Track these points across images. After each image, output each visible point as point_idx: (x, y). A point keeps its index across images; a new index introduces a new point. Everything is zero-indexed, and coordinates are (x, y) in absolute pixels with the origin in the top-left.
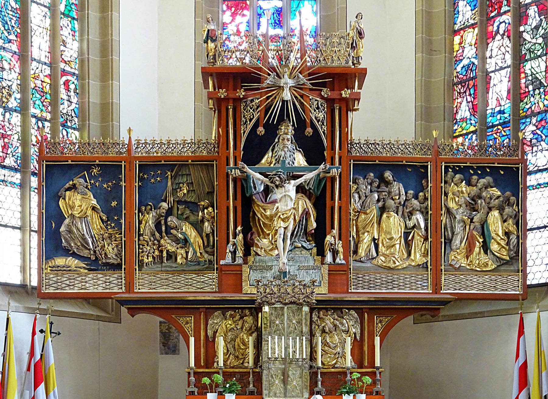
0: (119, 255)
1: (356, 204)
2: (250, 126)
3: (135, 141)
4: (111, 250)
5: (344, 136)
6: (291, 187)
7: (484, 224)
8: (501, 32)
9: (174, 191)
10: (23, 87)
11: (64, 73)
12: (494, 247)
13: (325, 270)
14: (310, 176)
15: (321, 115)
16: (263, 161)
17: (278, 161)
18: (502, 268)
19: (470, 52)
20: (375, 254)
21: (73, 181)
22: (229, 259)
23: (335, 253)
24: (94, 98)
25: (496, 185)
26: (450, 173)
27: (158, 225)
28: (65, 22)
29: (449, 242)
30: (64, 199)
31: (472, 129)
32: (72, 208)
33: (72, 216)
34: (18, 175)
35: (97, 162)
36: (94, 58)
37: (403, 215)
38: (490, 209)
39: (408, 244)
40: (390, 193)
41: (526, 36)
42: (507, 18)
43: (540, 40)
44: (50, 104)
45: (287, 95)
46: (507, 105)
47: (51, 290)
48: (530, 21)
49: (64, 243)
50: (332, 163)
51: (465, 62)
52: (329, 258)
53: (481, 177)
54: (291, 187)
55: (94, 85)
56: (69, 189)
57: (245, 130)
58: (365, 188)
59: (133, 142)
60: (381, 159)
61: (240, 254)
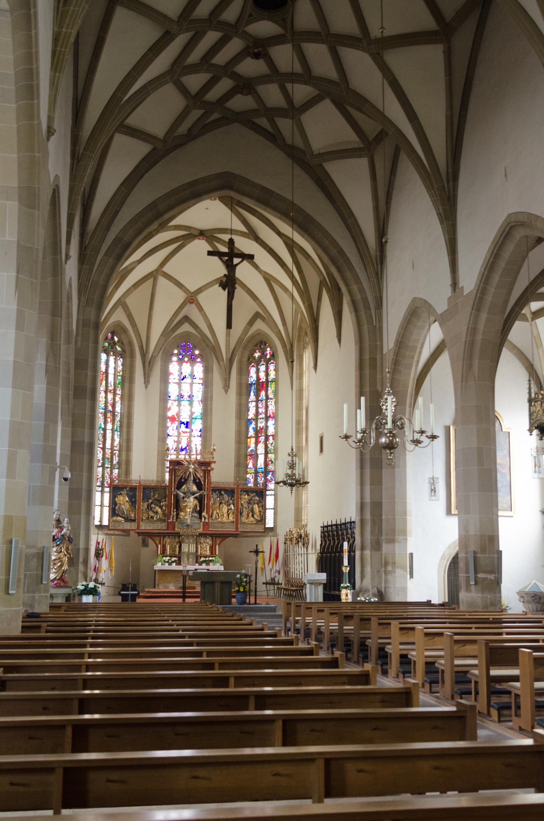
0: (135, 517)
1: (212, 501)
2: (179, 478)
4: (133, 515)
5: (209, 480)
6: (192, 499)
7: (252, 509)
8: (262, 442)
9: (154, 496)
10: (104, 458)
11: (115, 450)
12: (255, 516)
13: (202, 524)
14: (197, 495)
15: (201, 475)
16: (183, 488)
17: (188, 488)
18: (258, 523)
19: (252, 446)
20: (217, 517)
22: (171, 520)
23: (205, 518)
24: (124, 458)
25: (257, 495)
26: (242, 492)
27: (148, 507)
28: (116, 433)
29: (241, 514)
31: (253, 472)
32: (120, 501)
33: (120, 504)
34: (100, 488)
36: (124, 444)
37: (227, 506)
38: (254, 504)
39: (228, 515)
40: (223, 498)
41: (269, 446)
42: (263, 438)
43: (273, 448)
44: (110, 462)
45: (191, 470)
46: (263, 466)
47: (112, 528)
48: (270, 441)
49: (117, 513)
50: (205, 490)
51: (251, 449)
52: (203, 520)
53: (252, 493)
54: (192, 499)
55: (124, 453)
57: (178, 479)
58: (215, 496)
60: (221, 488)
61: (175, 518)
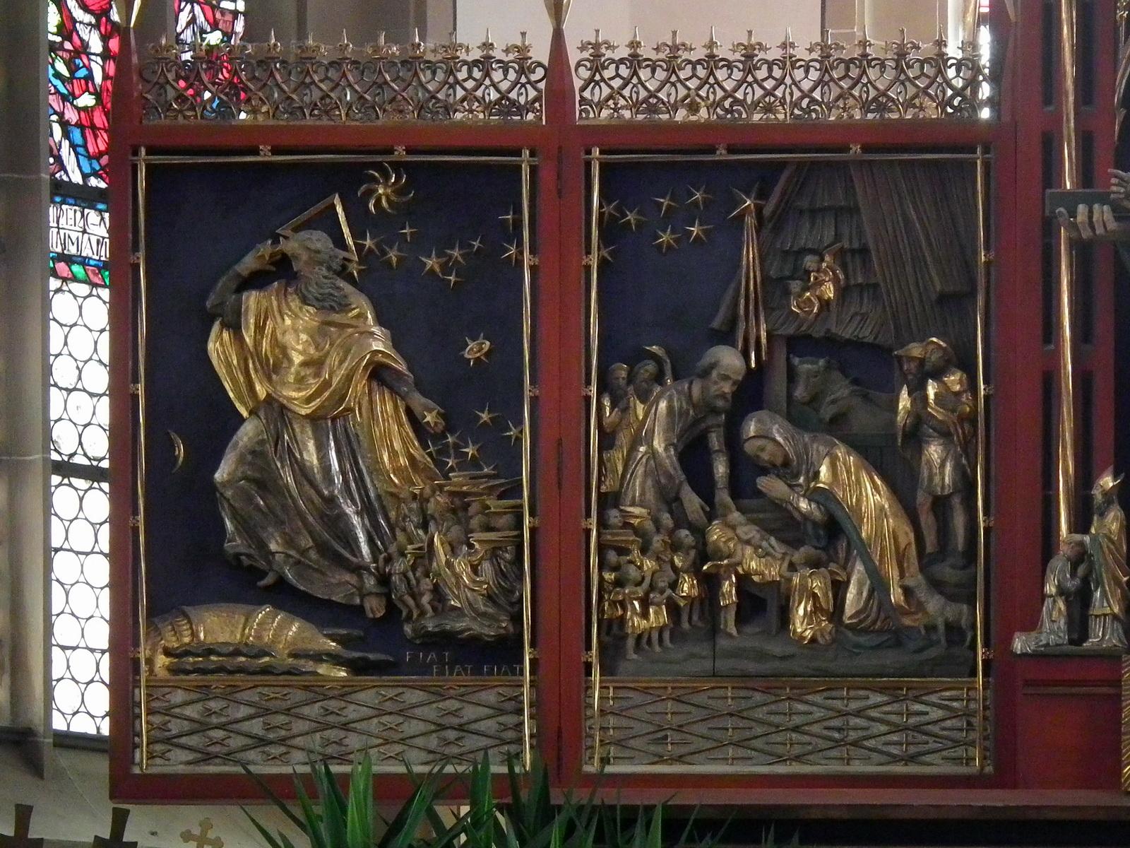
3: (583, 48)
21: (276, 241)
30: (235, 327)
32: (272, 369)
33: (276, 411)
35: (400, 153)
47: (177, 763)
49: (235, 543)
56: (257, 280)
59: (574, 56)
